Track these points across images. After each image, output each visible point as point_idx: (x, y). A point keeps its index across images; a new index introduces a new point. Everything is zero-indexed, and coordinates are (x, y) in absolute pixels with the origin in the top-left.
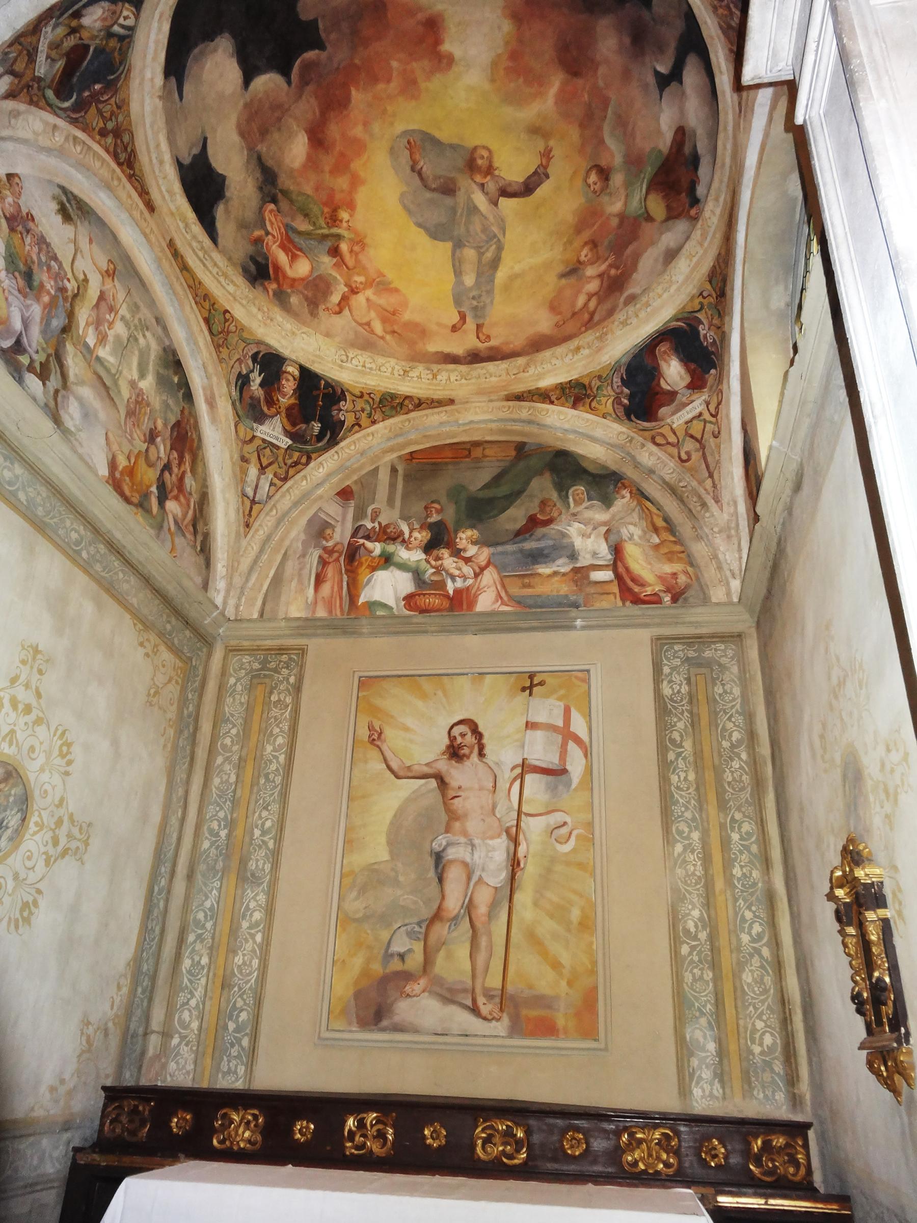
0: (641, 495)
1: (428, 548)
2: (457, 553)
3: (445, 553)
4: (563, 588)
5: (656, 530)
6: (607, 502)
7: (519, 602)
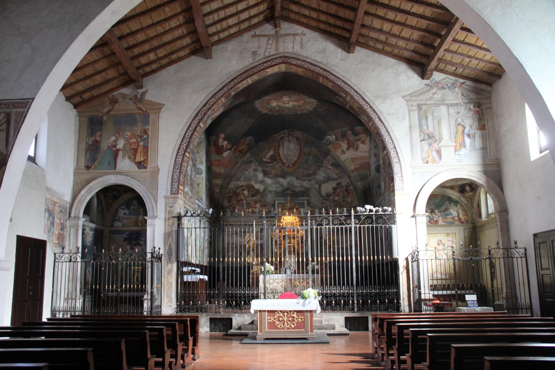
0: (461, 205)
1: (431, 213)
2: (435, 214)
3: (433, 214)
4: (450, 220)
5: (464, 211)
6: (457, 206)
7: (445, 222)
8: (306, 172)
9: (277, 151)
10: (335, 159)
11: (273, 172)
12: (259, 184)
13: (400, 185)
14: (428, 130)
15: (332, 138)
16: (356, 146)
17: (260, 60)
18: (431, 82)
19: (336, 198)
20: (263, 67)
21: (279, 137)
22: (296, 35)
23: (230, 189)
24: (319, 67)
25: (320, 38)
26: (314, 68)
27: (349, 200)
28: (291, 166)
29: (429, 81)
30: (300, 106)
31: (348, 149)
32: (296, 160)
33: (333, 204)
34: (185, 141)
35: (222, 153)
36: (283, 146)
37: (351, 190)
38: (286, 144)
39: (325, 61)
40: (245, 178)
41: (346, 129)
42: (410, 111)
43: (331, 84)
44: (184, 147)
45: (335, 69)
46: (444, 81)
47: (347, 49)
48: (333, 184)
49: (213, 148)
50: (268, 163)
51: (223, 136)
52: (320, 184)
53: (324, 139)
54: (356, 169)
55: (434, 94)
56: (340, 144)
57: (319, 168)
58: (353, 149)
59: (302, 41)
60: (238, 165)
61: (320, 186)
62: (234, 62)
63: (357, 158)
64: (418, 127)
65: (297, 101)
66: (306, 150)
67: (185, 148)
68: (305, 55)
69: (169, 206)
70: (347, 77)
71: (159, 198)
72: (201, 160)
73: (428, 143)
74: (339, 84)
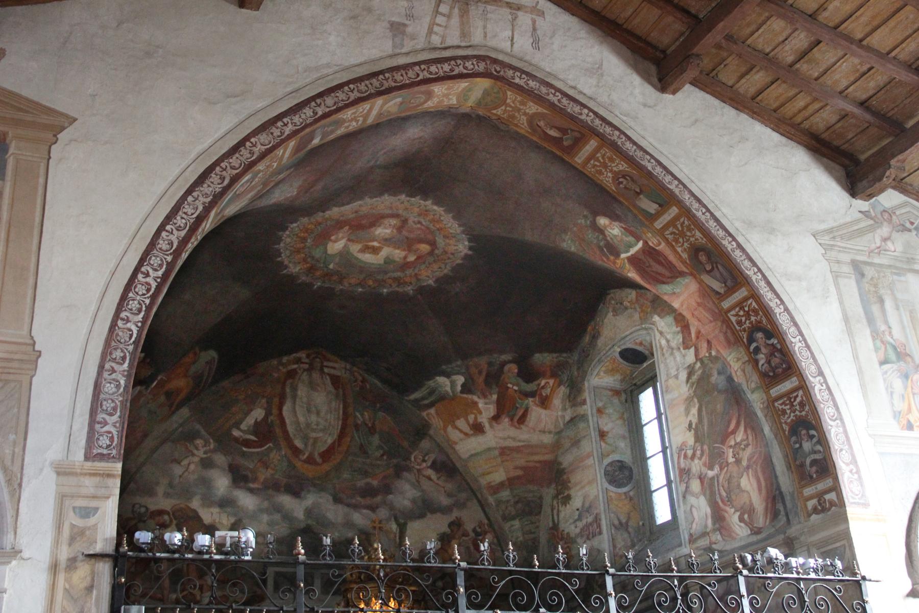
8: (361, 483)
9: (275, 411)
10: (441, 450)
11: (264, 475)
12: (215, 510)
13: (855, 487)
14: (890, 333)
15: (453, 384)
16: (520, 412)
17: (416, 51)
18: (873, 207)
20: (426, 74)
21: (285, 370)
22: (519, 8)
24: (590, 110)
25: (583, 34)
26: (577, 109)
28: (316, 456)
29: (867, 203)
30: (405, 266)
31: (496, 418)
32: (334, 443)
34: (155, 261)
36: (294, 397)
38: (302, 391)
39: (603, 98)
40: (171, 485)
41: (504, 357)
42: (836, 276)
43: (623, 166)
44: (149, 280)
45: (632, 124)
46: (903, 211)
47: (655, 80)
50: (247, 443)
52: (403, 520)
53: (419, 386)
54: (511, 482)
55: (885, 240)
56: (475, 404)
57: (399, 471)
58: (512, 420)
59: (534, 29)
62: (332, 38)
63: (517, 450)
64: (864, 321)
65: (409, 244)
66: (362, 416)
67: (154, 285)
68: (548, 70)
69: (74, 508)
70: (666, 153)
71: (29, 471)
73: (899, 371)
74: (650, 168)
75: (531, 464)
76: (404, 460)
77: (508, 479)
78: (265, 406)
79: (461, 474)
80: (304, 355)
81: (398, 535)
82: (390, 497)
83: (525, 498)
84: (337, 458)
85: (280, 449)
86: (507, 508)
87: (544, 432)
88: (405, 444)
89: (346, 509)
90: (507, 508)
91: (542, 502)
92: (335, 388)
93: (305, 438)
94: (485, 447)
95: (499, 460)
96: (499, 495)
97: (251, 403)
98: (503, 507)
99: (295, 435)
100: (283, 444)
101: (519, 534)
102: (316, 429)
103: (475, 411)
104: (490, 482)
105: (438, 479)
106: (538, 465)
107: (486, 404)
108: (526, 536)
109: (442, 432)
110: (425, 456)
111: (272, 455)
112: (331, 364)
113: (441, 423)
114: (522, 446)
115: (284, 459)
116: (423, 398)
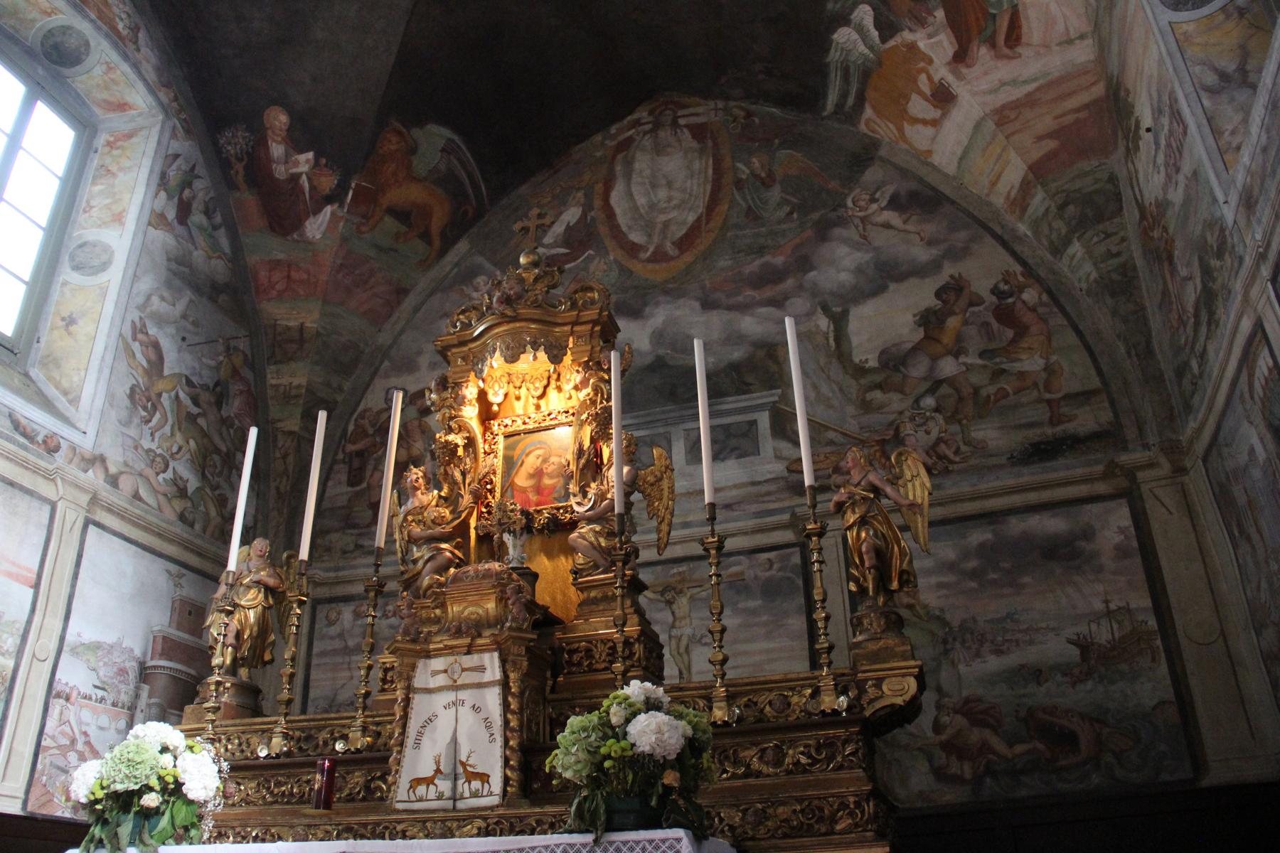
8: (753, 266)
9: (598, 203)
10: (904, 173)
15: (860, 29)
16: (1004, 24)
19: (948, 367)
21: (614, 143)
23: (362, 416)
27: (1032, 363)
28: (670, 249)
31: (961, 57)
32: (699, 220)
33: (929, 402)
35: (298, 225)
36: (628, 176)
37: (1033, 310)
38: (642, 163)
48: (922, 295)
49: (249, 199)
51: (279, 119)
53: (822, 72)
54: (1038, 172)
56: (912, 47)
57: (823, 232)
58: (993, 45)
60: (410, 302)
61: (839, 321)
63: (1029, 101)
72: (117, 208)
75: (1069, 119)
76: (834, 210)
77: (1030, 168)
78: (582, 200)
79: (953, 202)
80: (645, 114)
81: (831, 335)
82: (812, 274)
83: (1079, 190)
84: (703, 243)
85: (607, 253)
86: (1050, 225)
87: (1070, 42)
88: (834, 185)
89: (727, 315)
90: (1050, 225)
91: (1117, 186)
92: (699, 142)
93: (648, 227)
94: (970, 126)
95: (1001, 137)
96: (1030, 211)
97: (561, 203)
98: (1046, 230)
99: (630, 228)
100: (609, 243)
101: (1088, 267)
102: (666, 208)
103: (922, 64)
104: (1009, 193)
105: (905, 222)
106: (1082, 115)
107: (930, 36)
108: (1102, 266)
109: (903, 146)
110: (875, 193)
111: (592, 268)
112: (691, 110)
113: (891, 126)
114: (1038, 89)
115: (614, 266)
116: (844, 95)
